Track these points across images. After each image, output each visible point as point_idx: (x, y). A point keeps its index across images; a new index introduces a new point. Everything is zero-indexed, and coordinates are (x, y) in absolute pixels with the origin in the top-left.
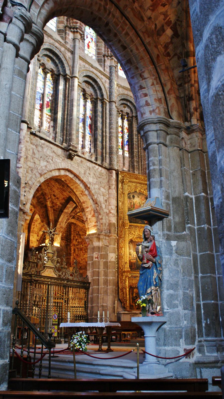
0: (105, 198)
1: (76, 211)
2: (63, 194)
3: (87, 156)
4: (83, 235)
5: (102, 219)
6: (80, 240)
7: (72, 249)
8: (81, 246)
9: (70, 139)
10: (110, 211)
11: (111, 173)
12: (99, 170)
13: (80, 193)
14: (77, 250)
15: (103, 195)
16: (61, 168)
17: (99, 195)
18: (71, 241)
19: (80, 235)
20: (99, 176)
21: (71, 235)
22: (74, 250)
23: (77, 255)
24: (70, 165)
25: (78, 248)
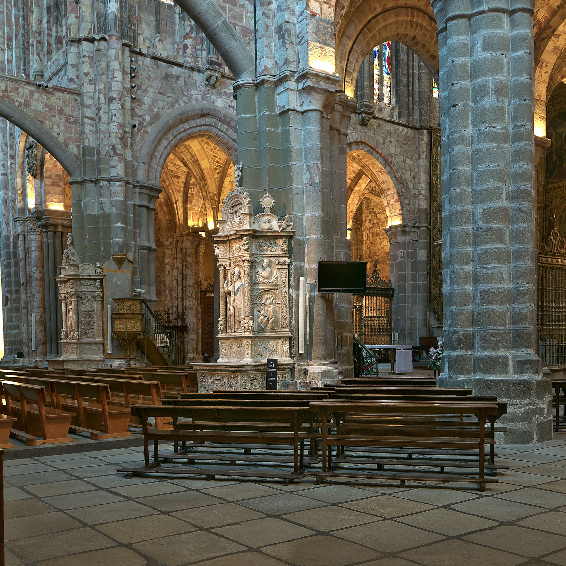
0: (413, 174)
1: (370, 187)
2: (352, 166)
3: (385, 115)
4: (379, 213)
5: (409, 204)
6: (375, 221)
7: (364, 235)
8: (378, 230)
9: (361, 94)
10: (419, 192)
11: (422, 134)
12: (404, 133)
13: (378, 170)
14: (371, 235)
15: (411, 170)
16: (352, 141)
17: (404, 171)
18: (362, 223)
19: (375, 213)
20: (404, 142)
21: (362, 215)
22: (368, 236)
23: (372, 243)
24: (363, 134)
25: (372, 233)
